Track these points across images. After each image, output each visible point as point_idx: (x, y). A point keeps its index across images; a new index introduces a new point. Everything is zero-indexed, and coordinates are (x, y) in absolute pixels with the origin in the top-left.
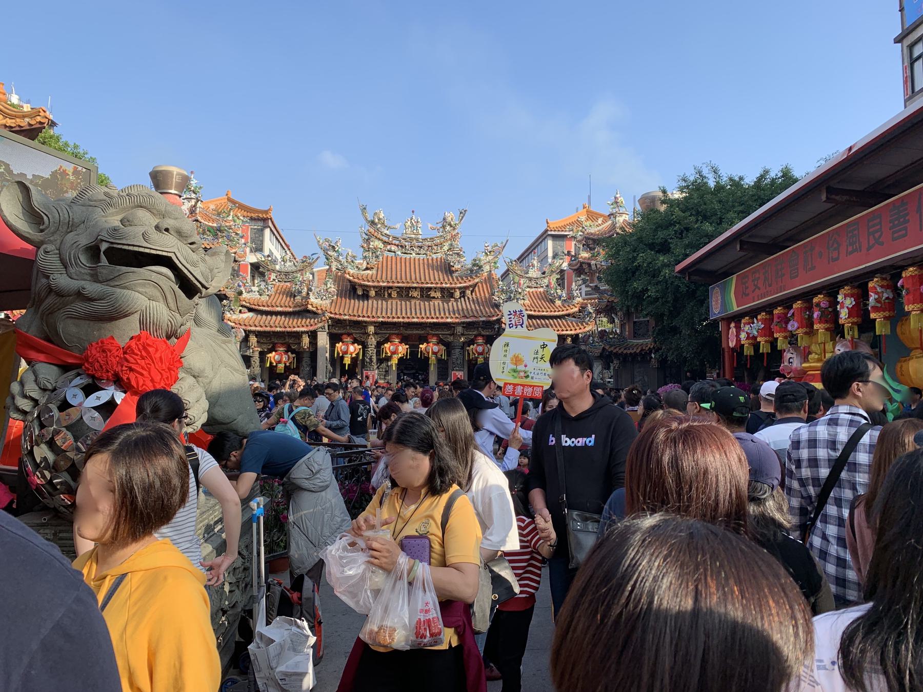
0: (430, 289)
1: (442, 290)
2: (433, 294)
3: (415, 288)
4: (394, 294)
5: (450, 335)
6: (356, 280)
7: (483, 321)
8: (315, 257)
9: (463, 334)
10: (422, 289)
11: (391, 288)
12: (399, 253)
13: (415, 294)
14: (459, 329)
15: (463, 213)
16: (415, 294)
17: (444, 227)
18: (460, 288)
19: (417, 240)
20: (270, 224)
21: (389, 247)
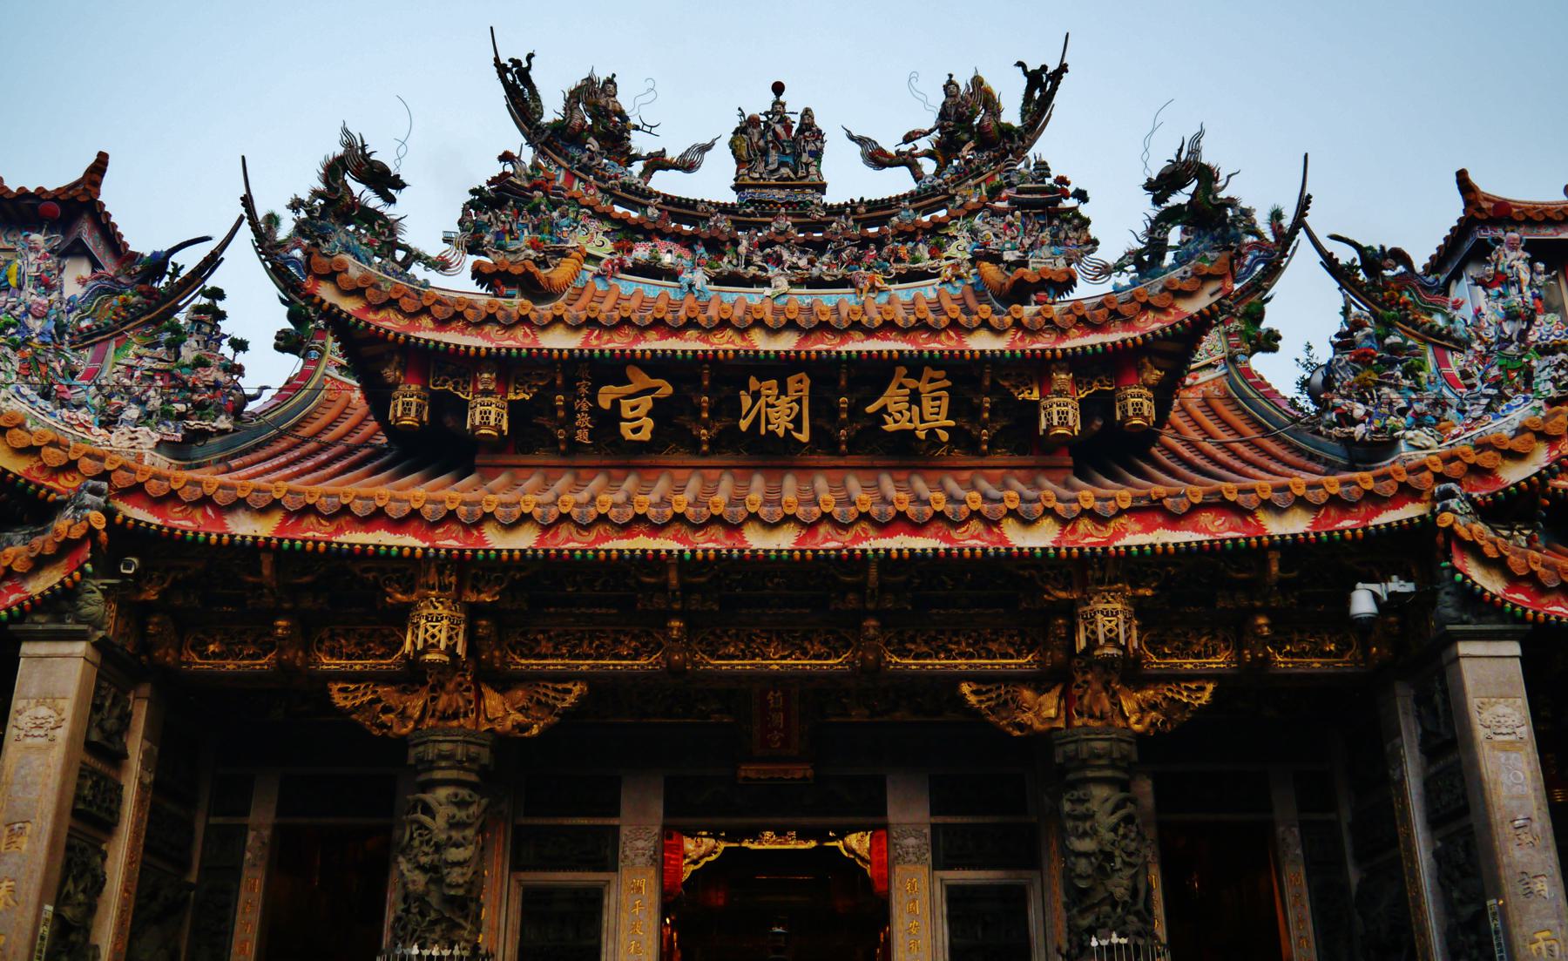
0: (876, 372)
1: (965, 374)
2: (896, 410)
3: (779, 368)
4: (638, 424)
5: (1040, 683)
6: (390, 322)
7: (1291, 547)
8: (189, 260)
9: (1130, 672)
10: (824, 372)
11: (613, 369)
12: (699, 278)
13: (779, 410)
14: (1109, 620)
15: (1042, 86)
16: (779, 410)
17: (944, 151)
18: (1081, 364)
19: (798, 209)
20: (89, 238)
21: (641, 252)
